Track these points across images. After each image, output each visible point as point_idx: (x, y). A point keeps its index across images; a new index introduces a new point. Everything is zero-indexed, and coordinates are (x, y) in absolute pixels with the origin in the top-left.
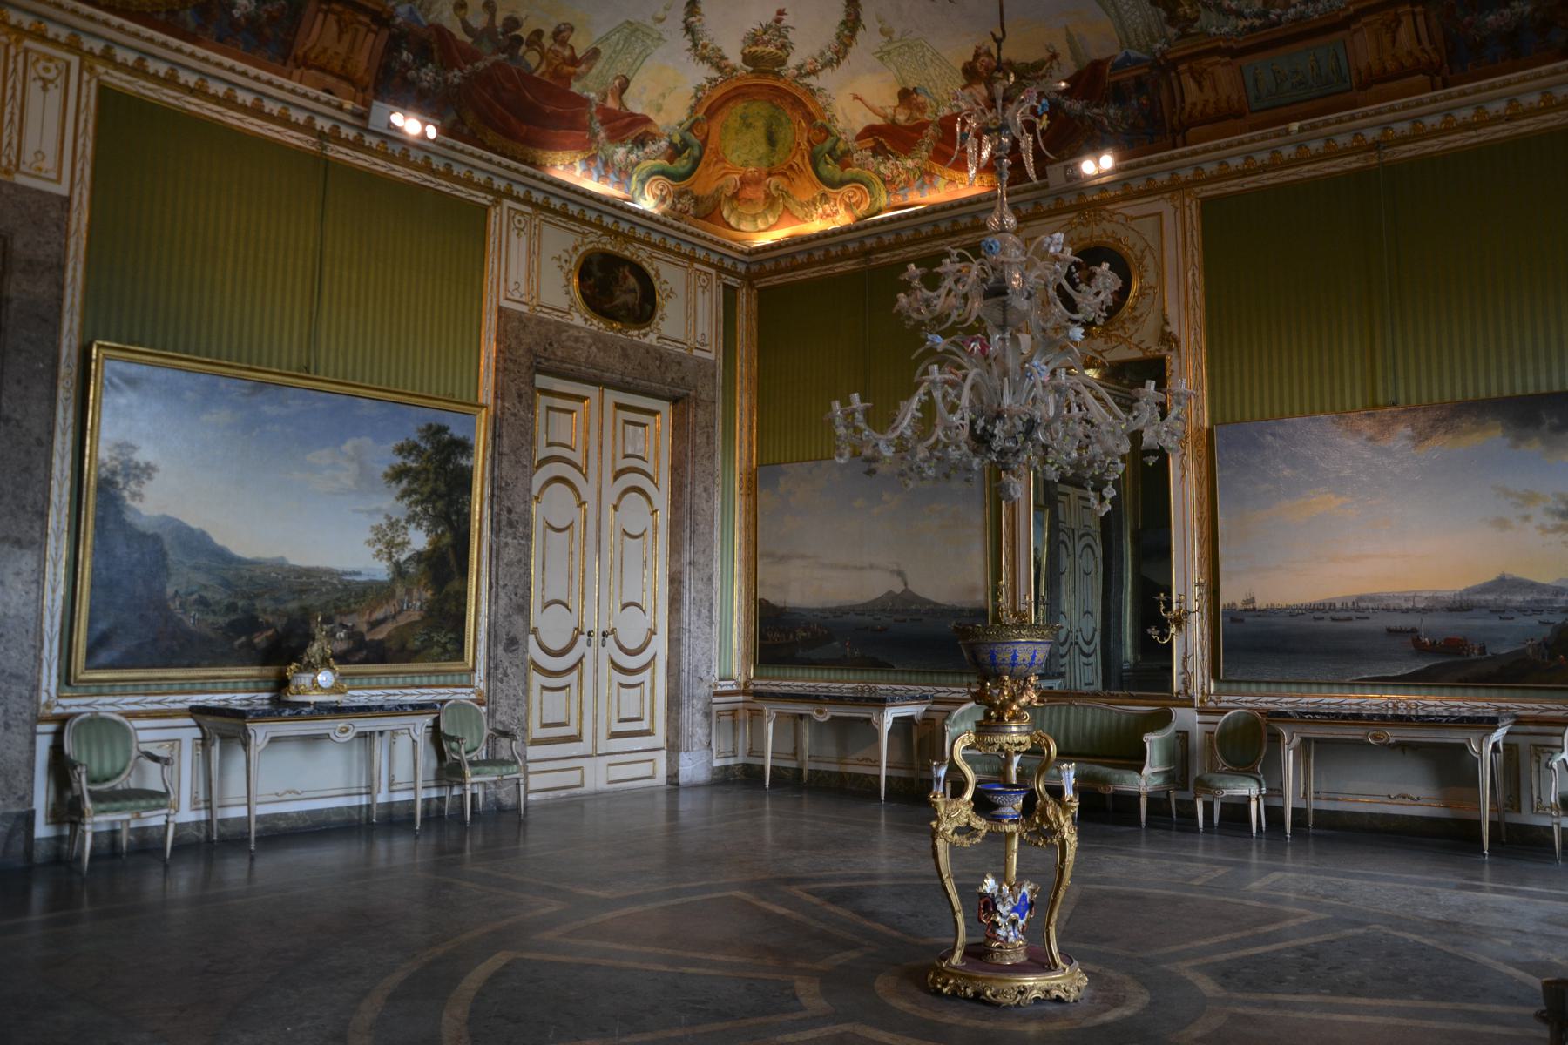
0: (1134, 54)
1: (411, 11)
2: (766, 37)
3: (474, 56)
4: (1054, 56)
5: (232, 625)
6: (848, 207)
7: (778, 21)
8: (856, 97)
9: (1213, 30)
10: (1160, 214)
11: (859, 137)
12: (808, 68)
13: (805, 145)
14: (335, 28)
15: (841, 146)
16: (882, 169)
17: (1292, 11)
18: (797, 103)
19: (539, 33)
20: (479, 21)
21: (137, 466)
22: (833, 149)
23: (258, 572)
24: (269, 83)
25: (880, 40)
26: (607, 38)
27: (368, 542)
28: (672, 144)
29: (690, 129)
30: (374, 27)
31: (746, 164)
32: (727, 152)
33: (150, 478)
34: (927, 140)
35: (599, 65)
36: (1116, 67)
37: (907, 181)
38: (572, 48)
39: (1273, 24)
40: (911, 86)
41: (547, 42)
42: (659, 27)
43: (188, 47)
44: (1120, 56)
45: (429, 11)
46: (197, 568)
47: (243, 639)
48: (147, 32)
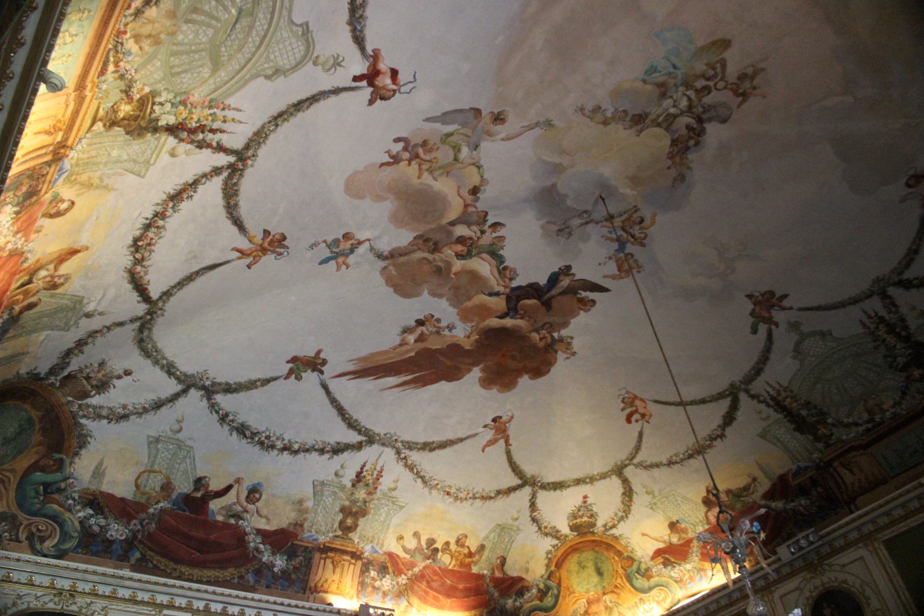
0: (802, 464)
2: (580, 513)
3: (413, 565)
4: (754, 479)
6: (658, 603)
7: (585, 502)
8: (644, 535)
9: (844, 437)
10: (862, 558)
11: (653, 558)
12: (610, 524)
13: (621, 571)
14: (331, 566)
15: (643, 566)
16: (672, 574)
17: (888, 413)
18: (609, 547)
19: (447, 543)
20: (411, 544)
22: (639, 569)
24: (297, 606)
25: (648, 498)
26: (487, 537)
28: (539, 590)
29: (549, 578)
30: (353, 561)
31: (587, 591)
32: (575, 586)
34: (695, 549)
35: (486, 553)
36: (795, 475)
37: (691, 578)
38: (468, 547)
39: (880, 424)
40: (674, 520)
41: (453, 547)
42: (516, 523)
43: (250, 595)
44: (794, 468)
45: (382, 545)
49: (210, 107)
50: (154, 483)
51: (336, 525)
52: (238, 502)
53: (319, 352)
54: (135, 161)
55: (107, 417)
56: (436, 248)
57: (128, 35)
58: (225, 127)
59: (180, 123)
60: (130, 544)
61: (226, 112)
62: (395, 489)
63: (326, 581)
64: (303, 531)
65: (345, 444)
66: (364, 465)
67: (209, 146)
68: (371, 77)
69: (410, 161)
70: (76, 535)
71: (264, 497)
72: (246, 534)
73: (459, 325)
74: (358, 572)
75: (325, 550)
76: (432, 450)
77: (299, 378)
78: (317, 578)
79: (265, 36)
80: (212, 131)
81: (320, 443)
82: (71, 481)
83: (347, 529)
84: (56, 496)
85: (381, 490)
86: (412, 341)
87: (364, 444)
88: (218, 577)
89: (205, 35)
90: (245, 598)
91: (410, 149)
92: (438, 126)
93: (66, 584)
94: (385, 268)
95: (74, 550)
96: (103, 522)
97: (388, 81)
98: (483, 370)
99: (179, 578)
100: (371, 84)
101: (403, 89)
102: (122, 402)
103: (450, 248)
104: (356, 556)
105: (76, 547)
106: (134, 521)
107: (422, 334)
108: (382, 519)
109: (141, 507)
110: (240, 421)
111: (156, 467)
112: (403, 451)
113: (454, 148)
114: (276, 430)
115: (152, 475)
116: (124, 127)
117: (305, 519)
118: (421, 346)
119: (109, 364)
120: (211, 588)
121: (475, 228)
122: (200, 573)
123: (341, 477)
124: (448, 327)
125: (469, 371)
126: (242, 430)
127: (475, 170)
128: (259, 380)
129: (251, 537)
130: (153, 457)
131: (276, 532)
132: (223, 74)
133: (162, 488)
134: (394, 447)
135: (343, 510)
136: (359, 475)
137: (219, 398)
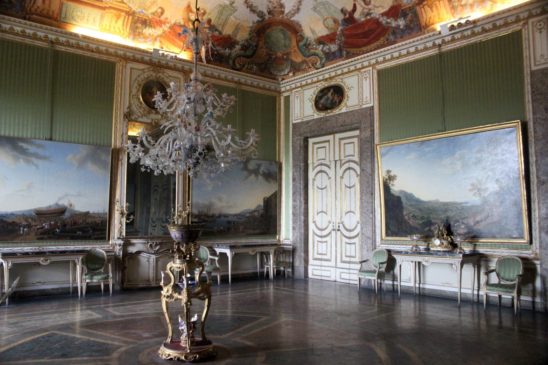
5: (423, 223)
14: (428, 9)
24: (414, 42)
27: (471, 190)
43: (396, 45)
47: (428, 228)
48: (386, 48)
50: (330, 23)
52: (364, 8)
55: (295, 13)
60: (340, 50)
63: (430, 18)
72: (378, 19)
78: (425, 20)
84: (310, 47)
90: (388, 50)
93: (327, 76)
95: (326, 62)
96: (327, 47)
99: (363, 54)
102: (292, 5)
105: (326, 60)
106: (336, 41)
109: (334, 34)
111: (325, 17)
115: (327, 20)
130: (319, 13)
131: (390, 10)
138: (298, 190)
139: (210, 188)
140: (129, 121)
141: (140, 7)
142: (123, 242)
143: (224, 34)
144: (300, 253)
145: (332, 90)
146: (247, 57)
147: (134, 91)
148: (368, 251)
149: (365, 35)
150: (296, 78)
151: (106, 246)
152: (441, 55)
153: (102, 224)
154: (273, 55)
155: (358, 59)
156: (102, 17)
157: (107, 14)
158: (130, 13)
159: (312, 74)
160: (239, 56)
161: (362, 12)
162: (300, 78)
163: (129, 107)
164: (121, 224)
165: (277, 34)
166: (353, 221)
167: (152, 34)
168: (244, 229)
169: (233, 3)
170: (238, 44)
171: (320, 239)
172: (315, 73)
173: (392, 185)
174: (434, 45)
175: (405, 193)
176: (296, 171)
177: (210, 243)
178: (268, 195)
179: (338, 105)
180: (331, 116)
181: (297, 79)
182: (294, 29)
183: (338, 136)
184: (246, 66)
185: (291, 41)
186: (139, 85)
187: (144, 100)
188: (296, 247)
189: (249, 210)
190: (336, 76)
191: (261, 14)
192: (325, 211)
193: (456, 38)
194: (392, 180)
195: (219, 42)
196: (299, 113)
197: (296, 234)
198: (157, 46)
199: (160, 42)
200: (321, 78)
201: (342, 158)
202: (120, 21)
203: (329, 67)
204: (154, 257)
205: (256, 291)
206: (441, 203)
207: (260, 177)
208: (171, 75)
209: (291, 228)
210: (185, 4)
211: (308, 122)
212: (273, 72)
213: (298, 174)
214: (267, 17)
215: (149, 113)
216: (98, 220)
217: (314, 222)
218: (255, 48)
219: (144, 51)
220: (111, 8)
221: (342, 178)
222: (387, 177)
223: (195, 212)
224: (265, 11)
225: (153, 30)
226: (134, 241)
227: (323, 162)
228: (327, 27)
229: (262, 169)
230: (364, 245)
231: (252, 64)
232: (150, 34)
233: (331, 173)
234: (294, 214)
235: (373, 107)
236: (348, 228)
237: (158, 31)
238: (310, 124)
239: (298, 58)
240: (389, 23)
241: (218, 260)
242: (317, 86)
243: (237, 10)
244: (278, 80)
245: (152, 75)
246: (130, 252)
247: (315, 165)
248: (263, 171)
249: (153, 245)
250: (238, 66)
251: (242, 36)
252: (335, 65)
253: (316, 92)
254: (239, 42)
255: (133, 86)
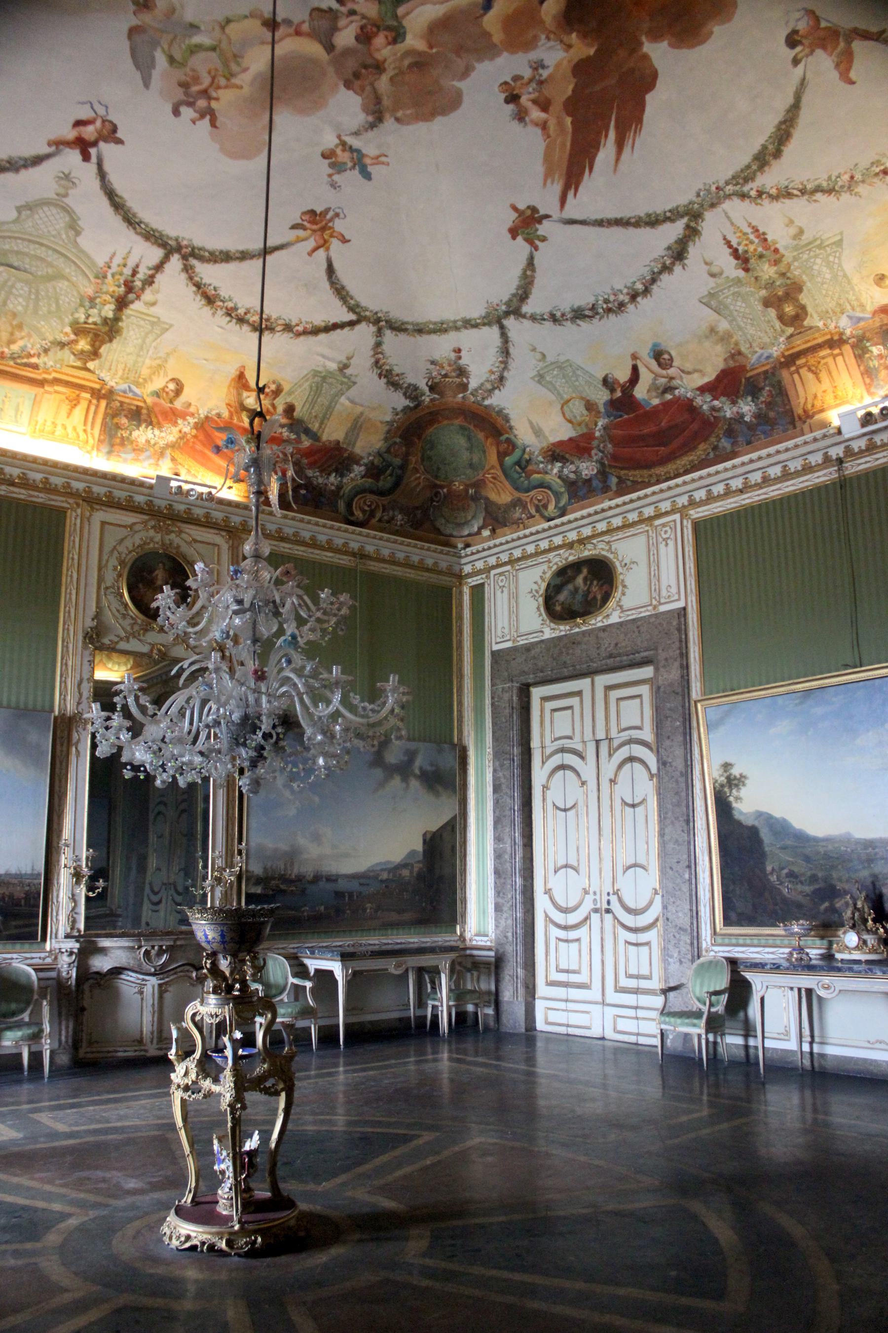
1: (850, 317)
5: (815, 892)
14: (810, 376)
21: (735, 778)
23: (830, 847)
24: (778, 452)
30: (837, 351)
33: (744, 785)
45: (862, 306)
46: (784, 848)
47: (827, 904)
48: (712, 470)
49: (105, 277)
50: (578, 409)
51: (778, 325)
52: (657, 376)
53: (514, 208)
54: (147, 334)
55: (494, 388)
56: (379, 67)
57: (6, 350)
58: (131, 264)
59: (117, 300)
60: (603, 474)
61: (114, 265)
62: (801, 232)
63: (815, 396)
64: (746, 357)
65: (676, 242)
66: (729, 244)
67: (152, 276)
68: (84, 146)
69: (210, 98)
70: (563, 490)
71: (673, 353)
72: (691, 401)
73: (534, 55)
74: (852, 361)
75: (790, 360)
76: (777, 154)
77: (544, 239)
78: (802, 401)
79: (30, 241)
80: (134, 273)
81: (652, 264)
82: (528, 449)
83: (797, 319)
84: (530, 468)
85: (786, 248)
86: (543, 115)
87: (693, 224)
88: (692, 461)
89: (22, 289)
90: (717, 473)
91: (191, 100)
92: (156, 74)
93: (573, 536)
94: (397, 120)
95: (569, 503)
97: (90, 128)
98: (656, 37)
99: (658, 482)
100: (95, 144)
101: (101, 111)
103: (378, 50)
104: (835, 342)
106: (593, 452)
107: (535, 102)
108: (828, 276)
109: (588, 437)
110: (568, 310)
111: (566, 397)
112: (746, 189)
113: (192, 52)
114: (604, 290)
115: (570, 404)
116: (103, 342)
117: (737, 344)
118: (557, 106)
119: (437, 357)
120: (679, 480)
121: (342, 23)
122: (674, 467)
123: (721, 274)
124: (536, 69)
125: (646, 57)
126: (579, 315)
127: (231, 29)
128: (525, 271)
129: (699, 401)
132: (68, 270)
133: (587, 409)
134: (728, 196)
135: (767, 303)
136: (735, 254)
137: (526, 309)
138: (507, 813)
139: (292, 812)
140: (96, 648)
141: (124, 379)
142: (77, 945)
143: (325, 438)
144: (513, 970)
145: (585, 571)
146: (381, 493)
147: (110, 577)
148: (681, 962)
149: (661, 438)
150: (497, 541)
151: (37, 957)
152: (843, 484)
153: (25, 898)
154: (442, 487)
155: (646, 496)
156: (36, 403)
157: (46, 395)
158: (102, 394)
159: (538, 532)
160: (360, 491)
161: (653, 384)
162: (507, 542)
163: (98, 616)
164: (75, 901)
165: (452, 439)
166: (643, 887)
167: (152, 442)
168: (376, 911)
169: (346, 366)
170: (358, 463)
171: (562, 934)
172: (544, 530)
173: (737, 799)
174: (827, 459)
175: (769, 819)
176: (502, 766)
177: (292, 946)
178: (434, 827)
179: (602, 606)
180: (584, 633)
181: (501, 544)
182: (491, 426)
183: (602, 680)
184: (378, 515)
185: (484, 452)
186: (122, 563)
187: (132, 598)
188: (503, 954)
189: (388, 862)
190: (593, 536)
191: (412, 392)
192: (575, 864)
193: (879, 443)
194: (737, 785)
195: (312, 459)
196: (506, 625)
197: (503, 922)
198: (165, 469)
199: (173, 459)
200: (558, 540)
201: (614, 733)
202: (79, 413)
203: (578, 515)
204: (153, 981)
205: (403, 1067)
206: (858, 842)
207: (414, 783)
208: (199, 538)
209: (491, 908)
210: (233, 372)
211: (528, 648)
212: (442, 528)
213: (507, 773)
214: (426, 399)
215: (146, 630)
216: (19, 893)
217: (548, 892)
218: (399, 472)
219: (133, 482)
220: (57, 381)
221: (613, 781)
222: (723, 779)
223: (257, 869)
224: (423, 385)
225: (157, 432)
226: (105, 943)
227: (567, 743)
228: (570, 421)
229: (418, 762)
230: (671, 947)
231: (393, 509)
232: (148, 441)
233: (587, 769)
234: (497, 872)
235: (684, 609)
236: (631, 905)
237: (168, 434)
238: (533, 652)
239: (502, 495)
240: (719, 410)
241: (312, 989)
242: (549, 561)
243: (355, 383)
244: (455, 547)
245: (152, 539)
246: (94, 969)
247: (548, 751)
248: (421, 768)
249: (153, 952)
250: (359, 514)
251: (368, 445)
252: (591, 510)
253: (548, 575)
254: (362, 458)
255: (106, 565)
